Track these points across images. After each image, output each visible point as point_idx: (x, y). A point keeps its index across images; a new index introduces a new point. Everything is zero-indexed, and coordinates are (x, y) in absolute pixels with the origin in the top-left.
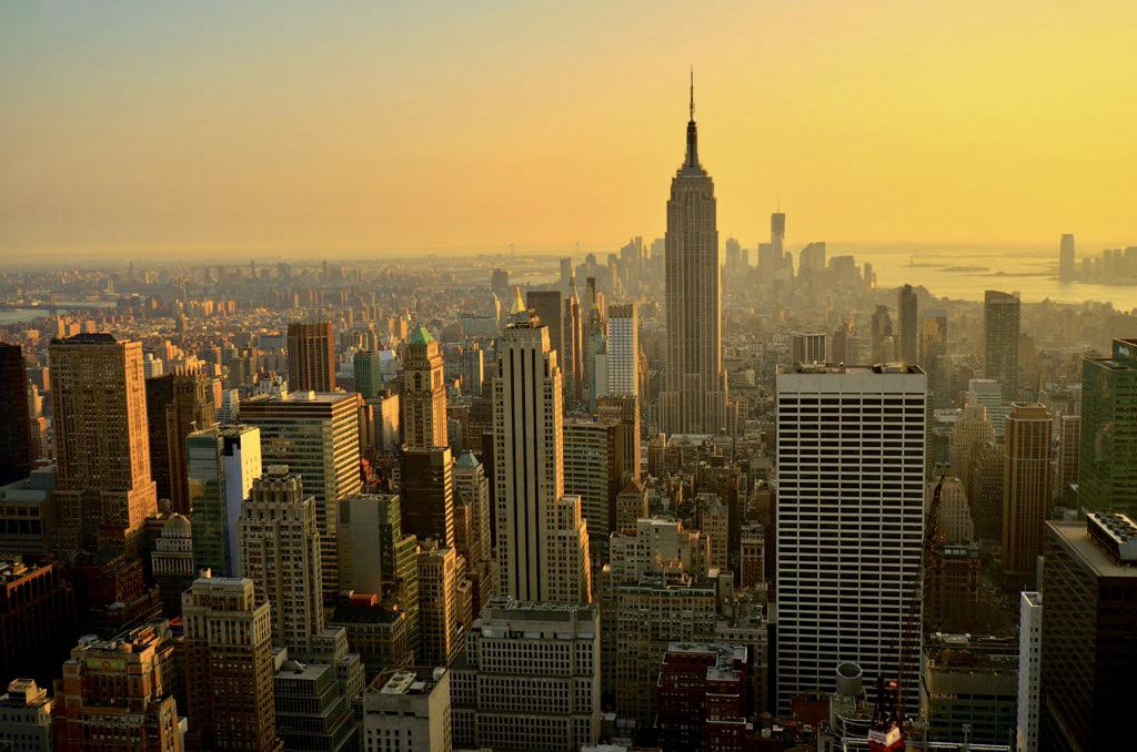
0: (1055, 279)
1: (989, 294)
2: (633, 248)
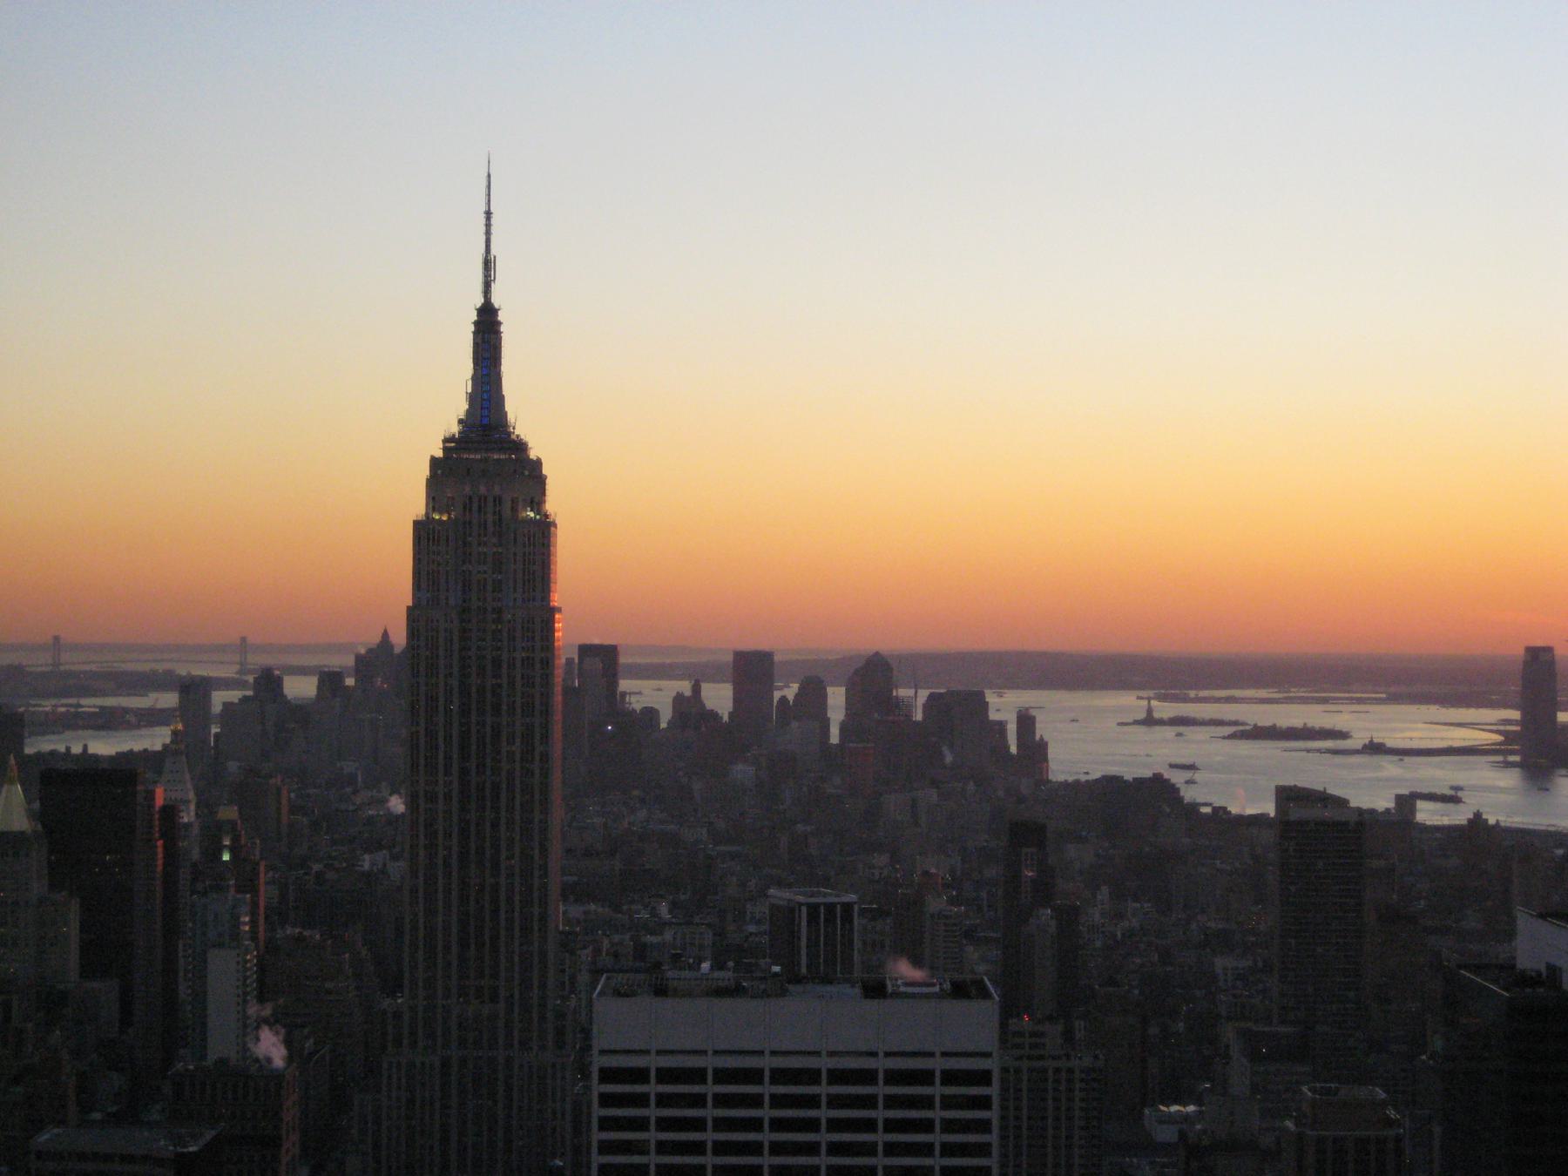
0: (1508, 765)
1: (1287, 796)
2: (373, 661)
